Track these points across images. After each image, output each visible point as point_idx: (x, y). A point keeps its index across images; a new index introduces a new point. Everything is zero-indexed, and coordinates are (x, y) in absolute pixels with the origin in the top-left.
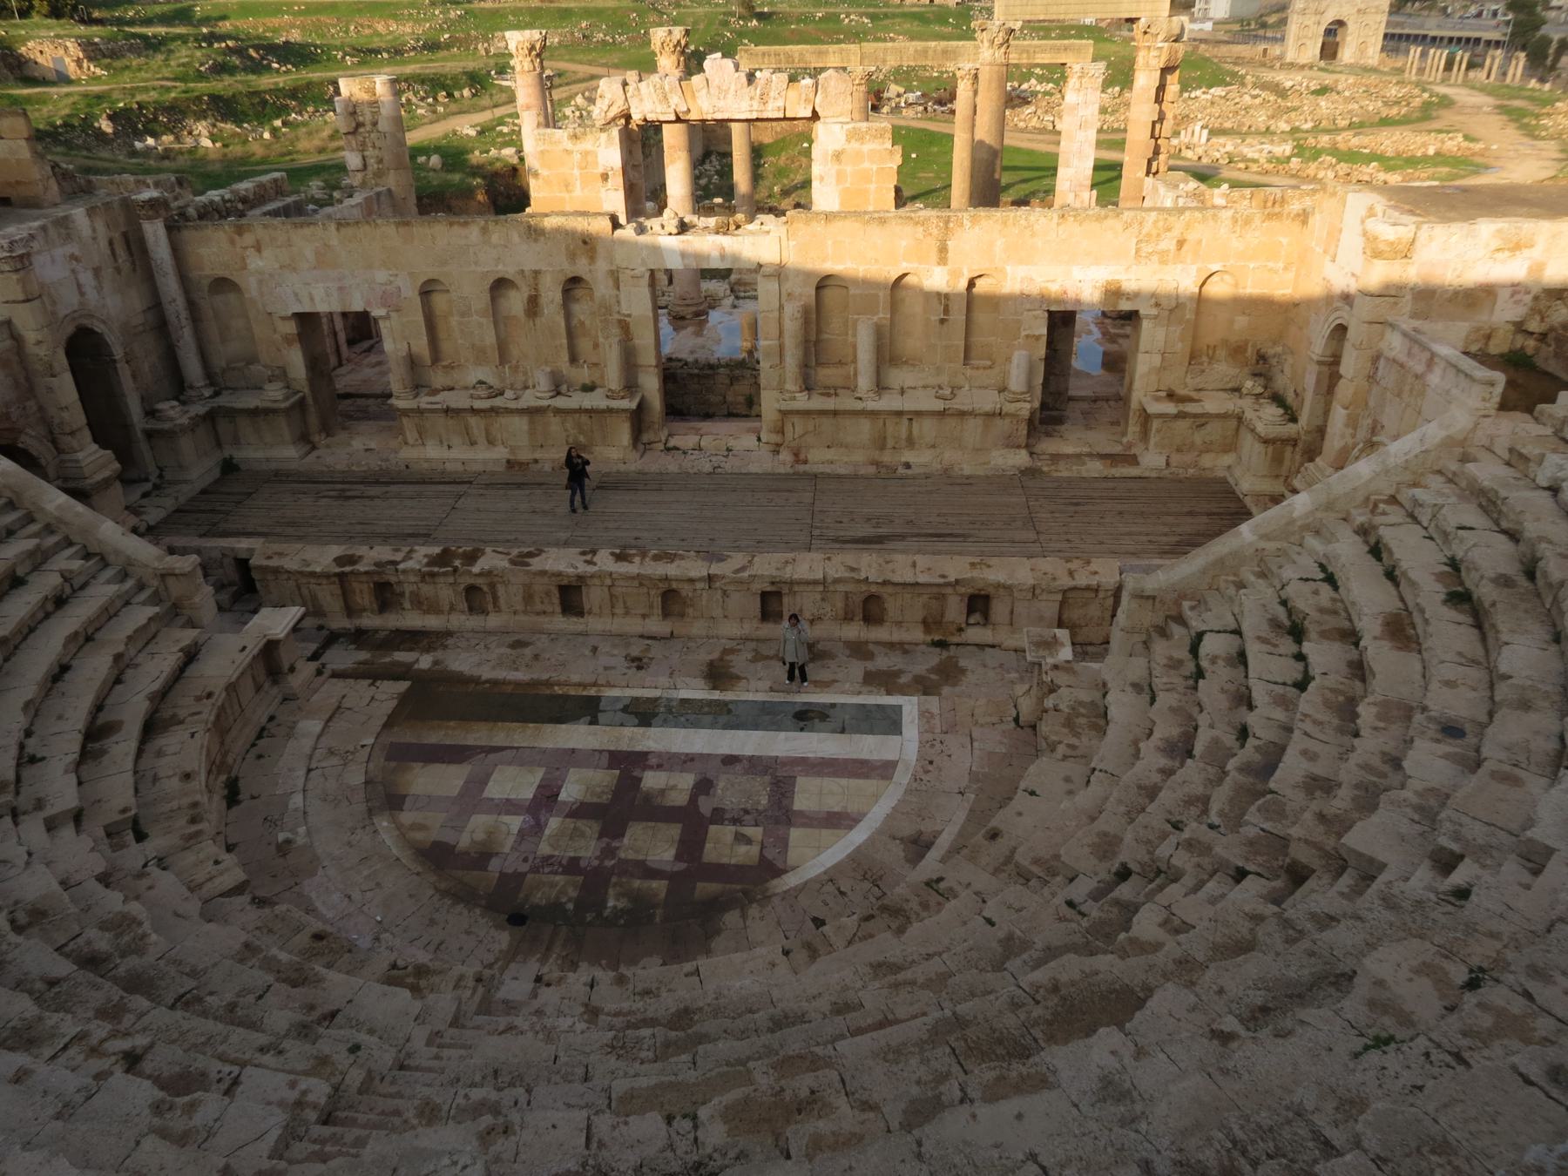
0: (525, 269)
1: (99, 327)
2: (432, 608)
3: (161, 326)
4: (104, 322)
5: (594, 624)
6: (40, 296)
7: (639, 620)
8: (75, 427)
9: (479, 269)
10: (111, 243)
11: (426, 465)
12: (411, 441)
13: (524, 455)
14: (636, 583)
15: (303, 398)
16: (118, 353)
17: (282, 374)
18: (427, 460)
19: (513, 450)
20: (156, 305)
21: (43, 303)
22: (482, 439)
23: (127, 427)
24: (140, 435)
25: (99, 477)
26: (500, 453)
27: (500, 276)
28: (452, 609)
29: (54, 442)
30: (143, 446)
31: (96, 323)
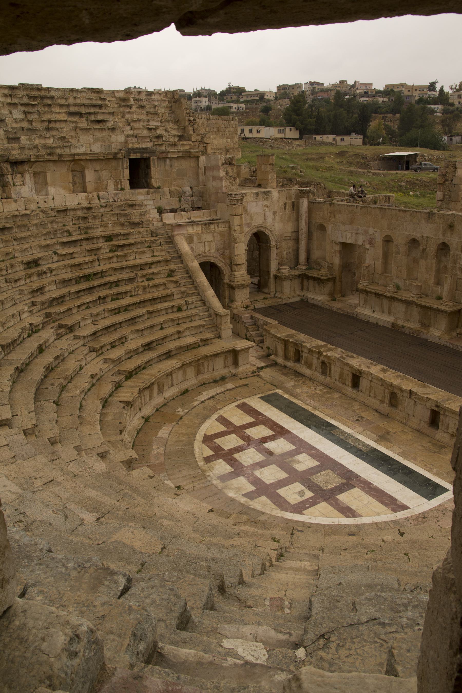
0: (424, 235)
1: (267, 232)
2: (310, 366)
3: (297, 240)
4: (271, 231)
5: (361, 396)
6: (241, 215)
7: (378, 402)
8: (238, 263)
9: (406, 233)
10: (285, 204)
11: (363, 317)
12: (361, 305)
13: (400, 323)
14: (380, 383)
15: (335, 278)
16: (273, 243)
17: (330, 268)
18: (364, 315)
19: (396, 318)
20: (297, 232)
21: (241, 218)
22: (386, 311)
23: (269, 272)
24: (272, 276)
25: (239, 283)
26: (391, 319)
27: (413, 237)
28: (316, 370)
29: (231, 267)
30: (272, 281)
31: (267, 230)
